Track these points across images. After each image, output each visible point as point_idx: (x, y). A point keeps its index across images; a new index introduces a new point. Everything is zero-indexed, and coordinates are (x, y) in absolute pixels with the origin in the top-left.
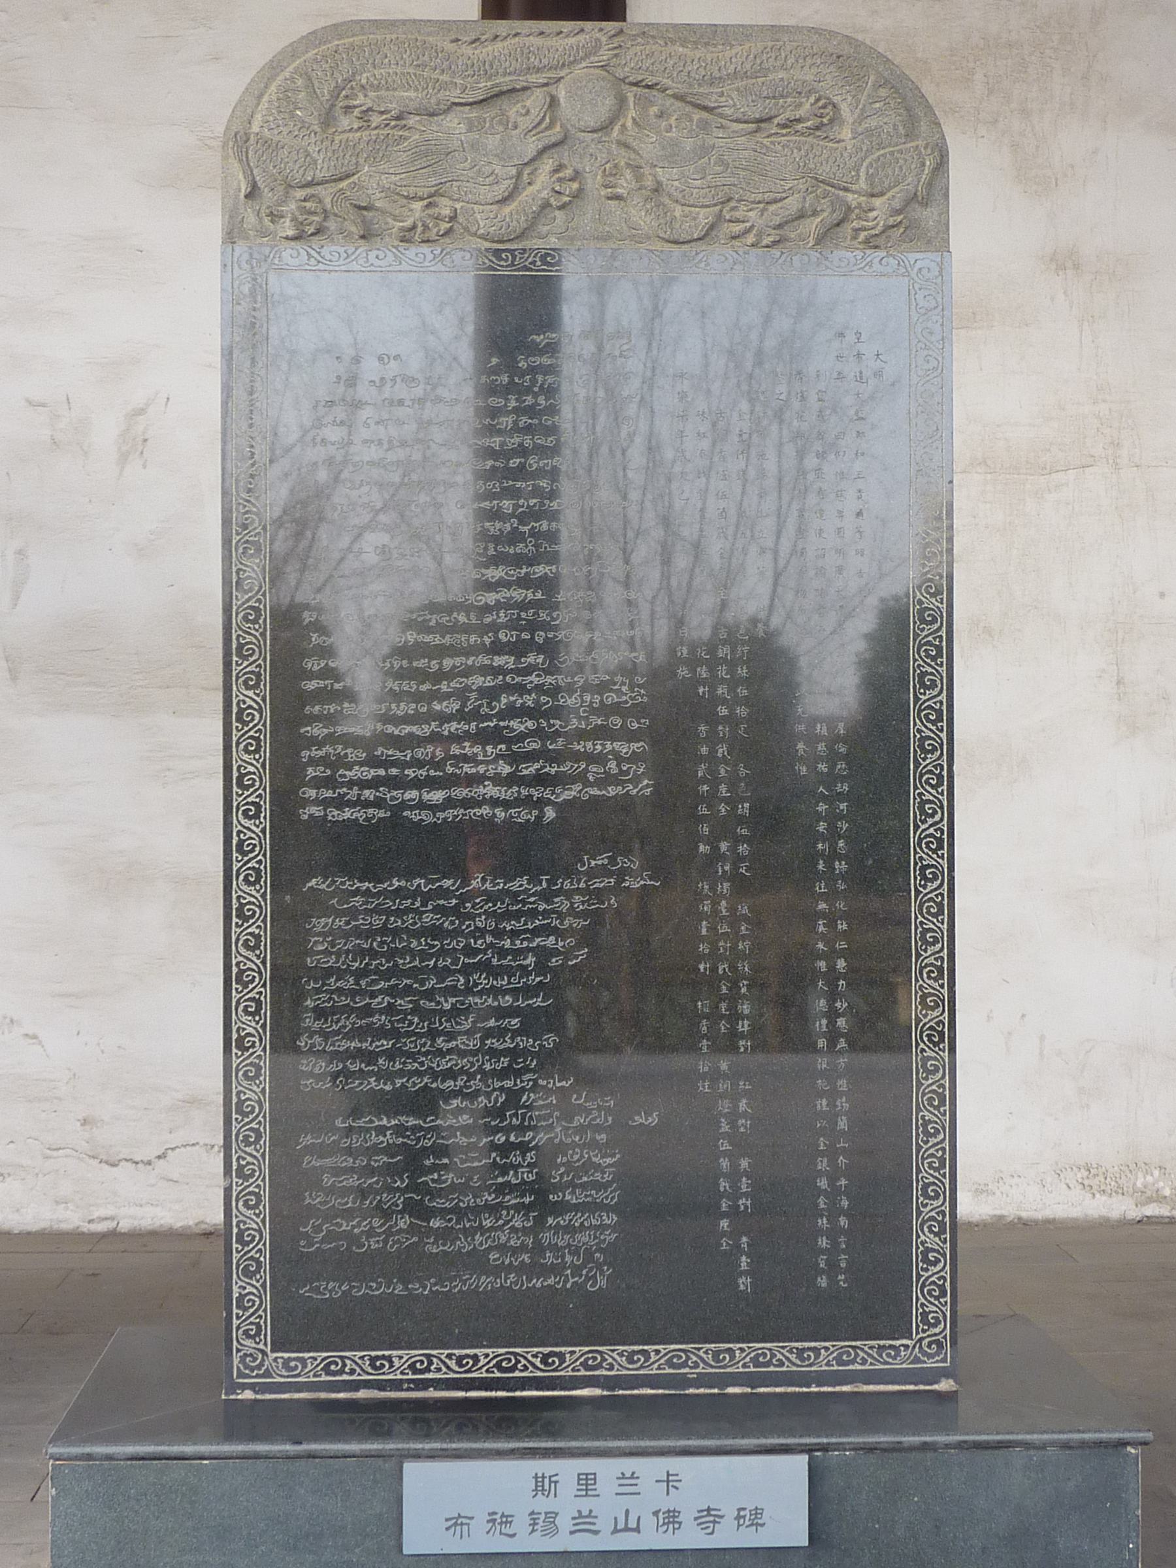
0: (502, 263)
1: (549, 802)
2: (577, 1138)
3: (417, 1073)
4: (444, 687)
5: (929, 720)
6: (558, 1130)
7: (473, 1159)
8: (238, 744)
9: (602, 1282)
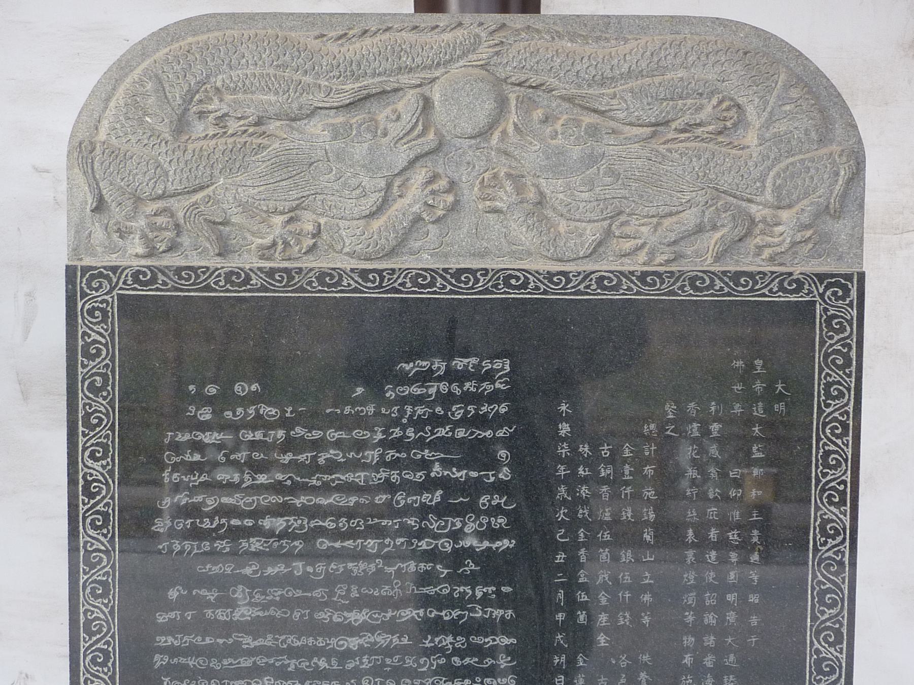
0: (369, 285)
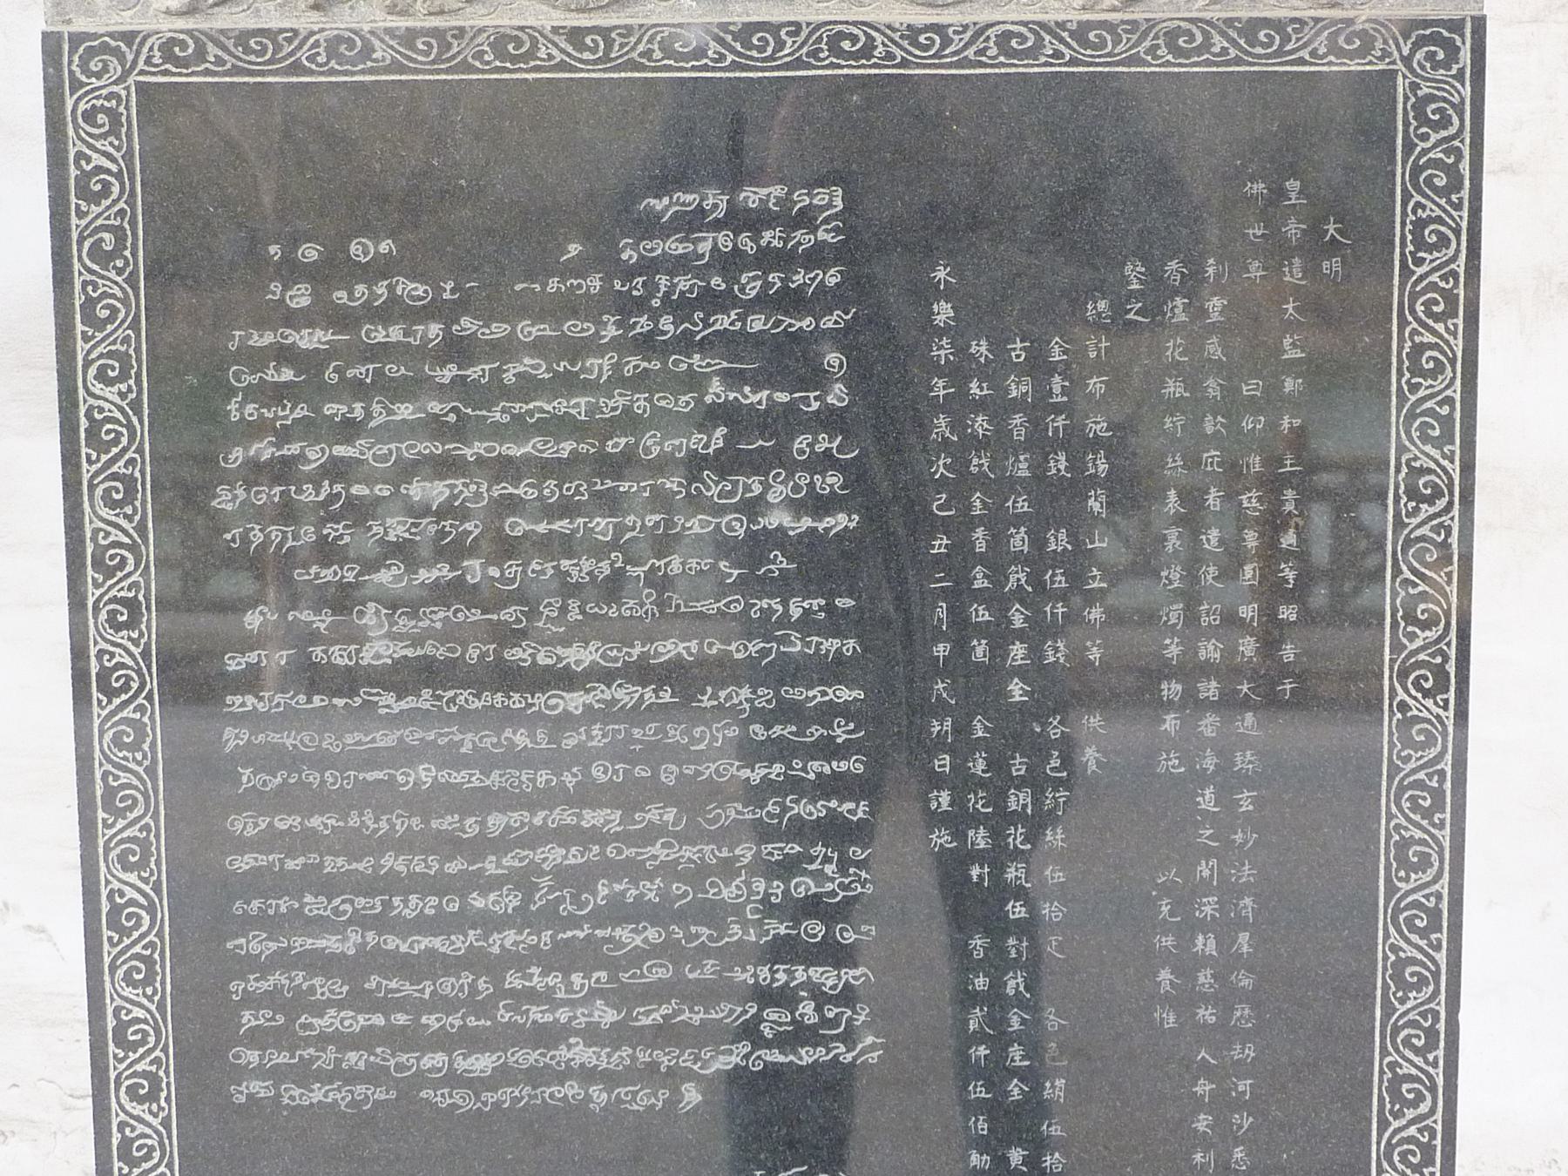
0: (586, 56)
1: (689, 1075)
4: (490, 866)
5: (1413, 928)
8: (113, 968)
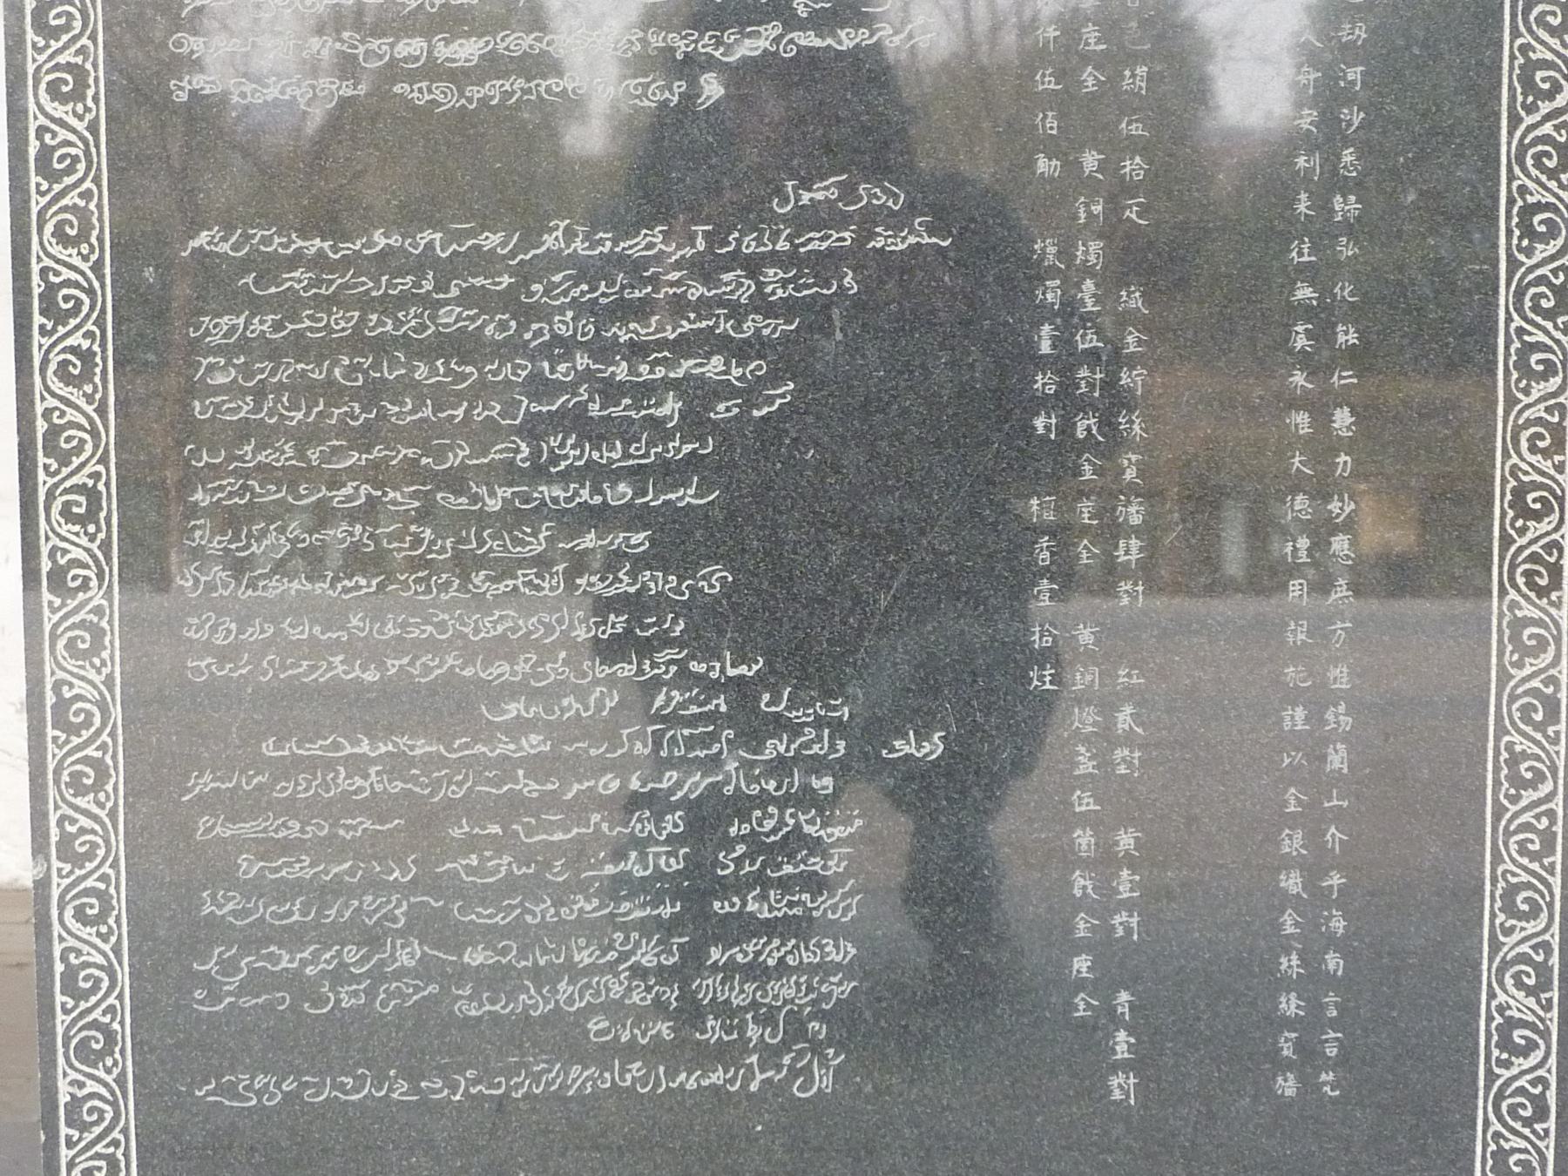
1: (710, 63)
2: (772, 785)
3: (432, 646)
6: (731, 766)
7: (550, 827)
9: (823, 1080)
